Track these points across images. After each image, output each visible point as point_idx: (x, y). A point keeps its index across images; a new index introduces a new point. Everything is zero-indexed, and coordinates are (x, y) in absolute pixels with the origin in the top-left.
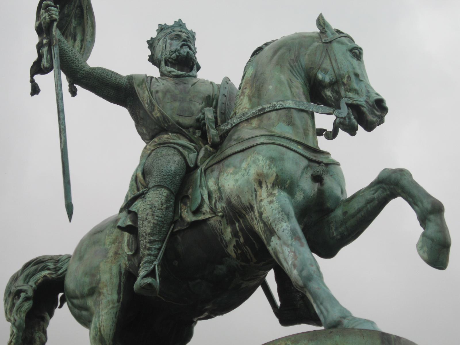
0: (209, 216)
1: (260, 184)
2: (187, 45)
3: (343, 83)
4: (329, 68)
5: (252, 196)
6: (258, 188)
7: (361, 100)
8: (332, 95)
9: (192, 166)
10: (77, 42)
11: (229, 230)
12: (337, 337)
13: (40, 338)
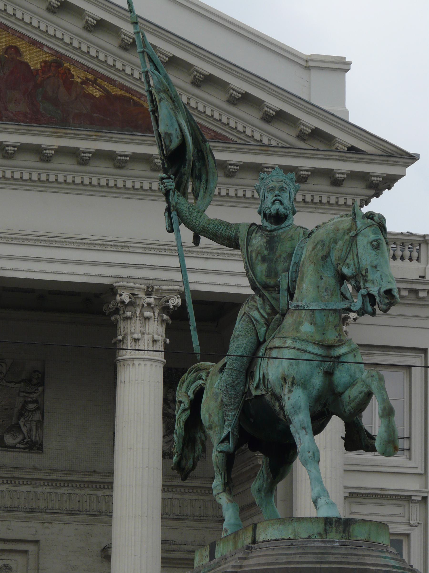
0: (264, 393)
1: (285, 380)
2: (278, 200)
3: (362, 275)
4: (351, 263)
5: (280, 389)
6: (284, 384)
7: (374, 290)
8: (356, 285)
9: (261, 340)
10: (202, 183)
11: (277, 404)
12: (296, 523)
13: (200, 438)
